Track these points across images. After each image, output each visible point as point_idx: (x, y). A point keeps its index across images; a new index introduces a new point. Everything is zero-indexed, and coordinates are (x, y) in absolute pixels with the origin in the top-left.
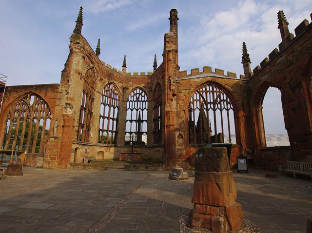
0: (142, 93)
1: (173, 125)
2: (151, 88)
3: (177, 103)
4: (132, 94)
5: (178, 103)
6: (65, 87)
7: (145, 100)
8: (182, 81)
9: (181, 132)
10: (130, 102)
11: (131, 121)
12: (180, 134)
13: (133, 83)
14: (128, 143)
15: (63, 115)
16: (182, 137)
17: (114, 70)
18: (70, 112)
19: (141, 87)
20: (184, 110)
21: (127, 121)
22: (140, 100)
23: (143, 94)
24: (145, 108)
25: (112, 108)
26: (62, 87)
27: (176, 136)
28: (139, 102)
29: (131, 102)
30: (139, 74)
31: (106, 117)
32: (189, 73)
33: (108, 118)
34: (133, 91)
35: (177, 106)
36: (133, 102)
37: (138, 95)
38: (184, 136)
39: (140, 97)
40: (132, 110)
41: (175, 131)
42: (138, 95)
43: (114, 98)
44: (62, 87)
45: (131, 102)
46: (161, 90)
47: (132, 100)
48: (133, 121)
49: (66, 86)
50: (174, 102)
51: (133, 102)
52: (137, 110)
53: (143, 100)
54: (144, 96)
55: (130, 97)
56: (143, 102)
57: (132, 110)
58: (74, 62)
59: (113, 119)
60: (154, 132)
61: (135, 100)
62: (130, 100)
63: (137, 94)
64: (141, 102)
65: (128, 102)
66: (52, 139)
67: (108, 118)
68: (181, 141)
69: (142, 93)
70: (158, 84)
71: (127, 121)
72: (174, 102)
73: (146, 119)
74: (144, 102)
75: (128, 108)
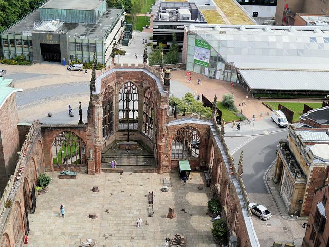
7: (136, 92)
13: (125, 78)
15: (94, 146)
23: (134, 87)
29: (123, 95)
37: (129, 88)
39: (131, 90)
42: (129, 88)
57: (124, 101)
69: (132, 86)
71: (120, 110)
72: (164, 140)
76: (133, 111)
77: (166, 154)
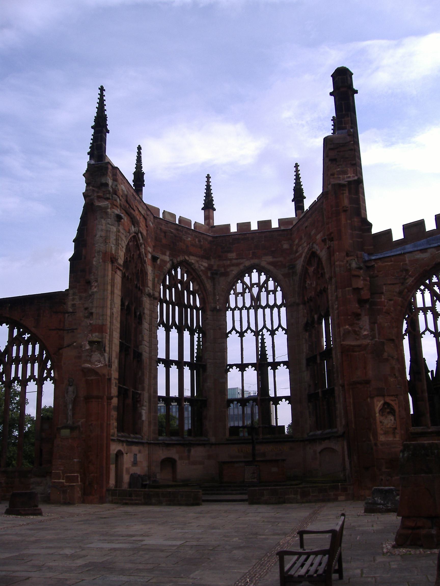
0: (266, 282)
1: (367, 382)
2: (293, 267)
3: (373, 322)
4: (239, 287)
5: (375, 323)
6: (81, 299)
7: (279, 302)
8: (380, 264)
9: (388, 399)
10: (233, 310)
11: (242, 367)
12: (385, 403)
14: (234, 430)
15: (87, 372)
16: (392, 412)
17: (184, 222)
18: (99, 362)
19: (263, 264)
20: (393, 340)
21: (231, 366)
22: (264, 303)
24: (280, 325)
25: (186, 334)
26: (73, 300)
27: (377, 409)
28: (260, 311)
29: (237, 313)
30: (254, 227)
31: (172, 362)
32: (398, 235)
33: (176, 363)
34: (241, 278)
35: (372, 330)
36: (244, 312)
37: (255, 290)
38: (396, 408)
39: (263, 295)
40: (242, 334)
41: (372, 398)
42: (255, 290)
43: (189, 306)
44: (73, 300)
45: (237, 313)
46: (323, 275)
47: (240, 305)
48: (247, 365)
49: (84, 295)
50: (365, 321)
51: (244, 312)
52: (257, 333)
53: (271, 303)
54: (274, 292)
55: (232, 298)
56: (272, 308)
57: (242, 334)
58: (99, 234)
59: (180, 364)
60: (312, 397)
61: (248, 305)
62: (233, 305)
63: (252, 285)
64: (268, 311)
65: (229, 314)
66: (65, 432)
67: (176, 363)
68: (389, 421)
69: (266, 282)
70: (313, 255)
71: (231, 366)
72: (365, 321)
73: (286, 359)
74: (275, 310)
75: (229, 328)
76: (275, 365)
77: (381, 393)
